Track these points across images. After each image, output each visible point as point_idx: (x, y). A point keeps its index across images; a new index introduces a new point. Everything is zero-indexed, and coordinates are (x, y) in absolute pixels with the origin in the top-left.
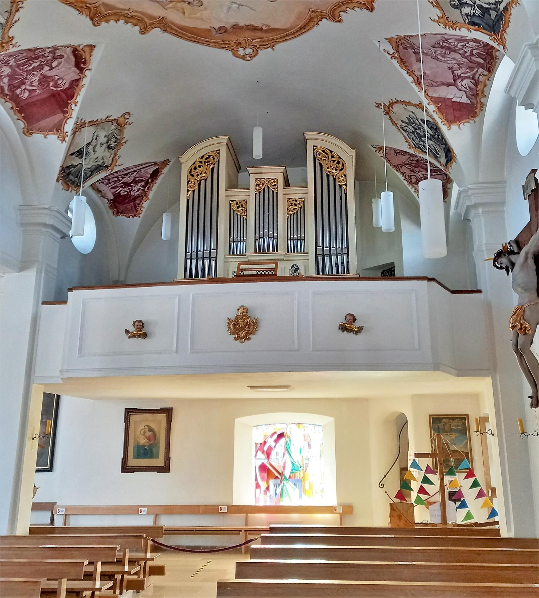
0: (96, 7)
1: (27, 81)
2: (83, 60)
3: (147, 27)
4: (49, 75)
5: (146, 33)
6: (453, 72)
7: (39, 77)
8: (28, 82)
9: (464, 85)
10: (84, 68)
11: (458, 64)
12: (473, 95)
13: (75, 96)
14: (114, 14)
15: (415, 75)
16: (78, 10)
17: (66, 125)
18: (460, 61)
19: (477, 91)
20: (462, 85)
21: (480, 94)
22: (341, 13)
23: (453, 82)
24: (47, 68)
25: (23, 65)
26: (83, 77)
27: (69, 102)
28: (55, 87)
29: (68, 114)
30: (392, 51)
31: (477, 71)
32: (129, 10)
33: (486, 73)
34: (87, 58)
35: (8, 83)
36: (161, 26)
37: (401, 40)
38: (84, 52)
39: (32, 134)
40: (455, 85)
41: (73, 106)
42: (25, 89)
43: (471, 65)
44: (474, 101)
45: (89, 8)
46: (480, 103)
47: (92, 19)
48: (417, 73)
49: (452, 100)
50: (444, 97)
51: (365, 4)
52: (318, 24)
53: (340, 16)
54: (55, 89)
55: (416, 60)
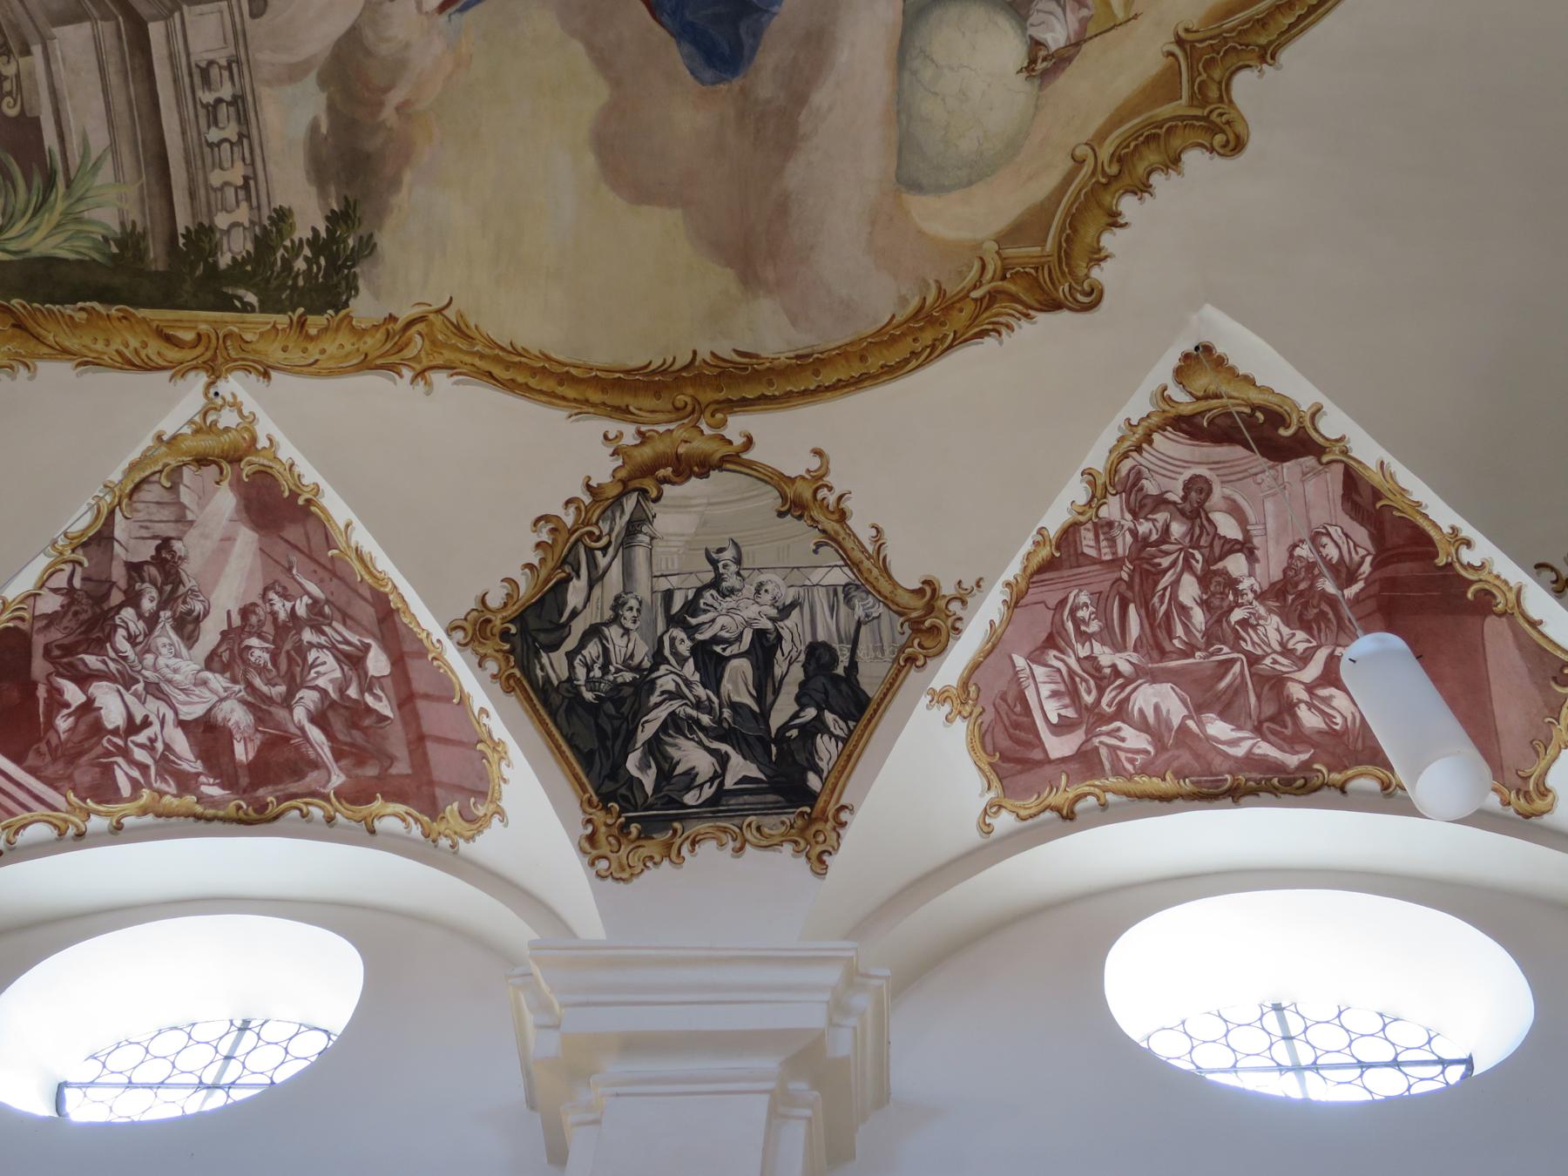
0: (1005, 269)
1: (1268, 661)
2: (1260, 416)
3: (1206, 118)
4: (1277, 574)
5: (1239, 128)
7: (1270, 611)
8: (1275, 662)
10: (1302, 428)
13: (1421, 521)
14: (1074, 222)
16: (982, 334)
17: (1545, 629)
24: (1236, 564)
25: (1162, 635)
26: (1345, 452)
27: (1441, 561)
28: (1351, 578)
29: (1500, 598)
32: (1079, 162)
34: (1255, 397)
35: (1239, 728)
36: (1232, 61)
38: (1217, 396)
39: (1549, 791)
41: (1466, 556)
42: (1310, 688)
45: (993, 297)
47: (1054, 306)
54: (1360, 585)
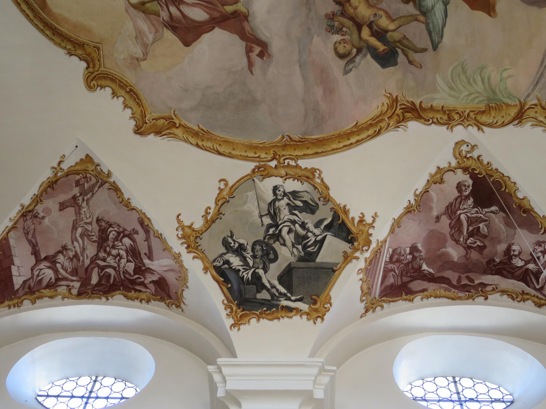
6: (59, 252)
9: (42, 272)
11: (76, 256)
12: (29, 288)
15: (35, 206)
18: (83, 256)
19: (38, 291)
20: (41, 269)
21: (34, 296)
22: (108, 91)
23: (43, 256)
30: (65, 166)
31: (72, 281)
33: (75, 292)
37: (96, 176)
40: (38, 260)
43: (81, 271)
44: (21, 292)
46: (20, 300)
48: (40, 208)
49: (12, 266)
50: (13, 254)
51: (146, 123)
52: (71, 55)
53: (102, 87)
55: (62, 201)
